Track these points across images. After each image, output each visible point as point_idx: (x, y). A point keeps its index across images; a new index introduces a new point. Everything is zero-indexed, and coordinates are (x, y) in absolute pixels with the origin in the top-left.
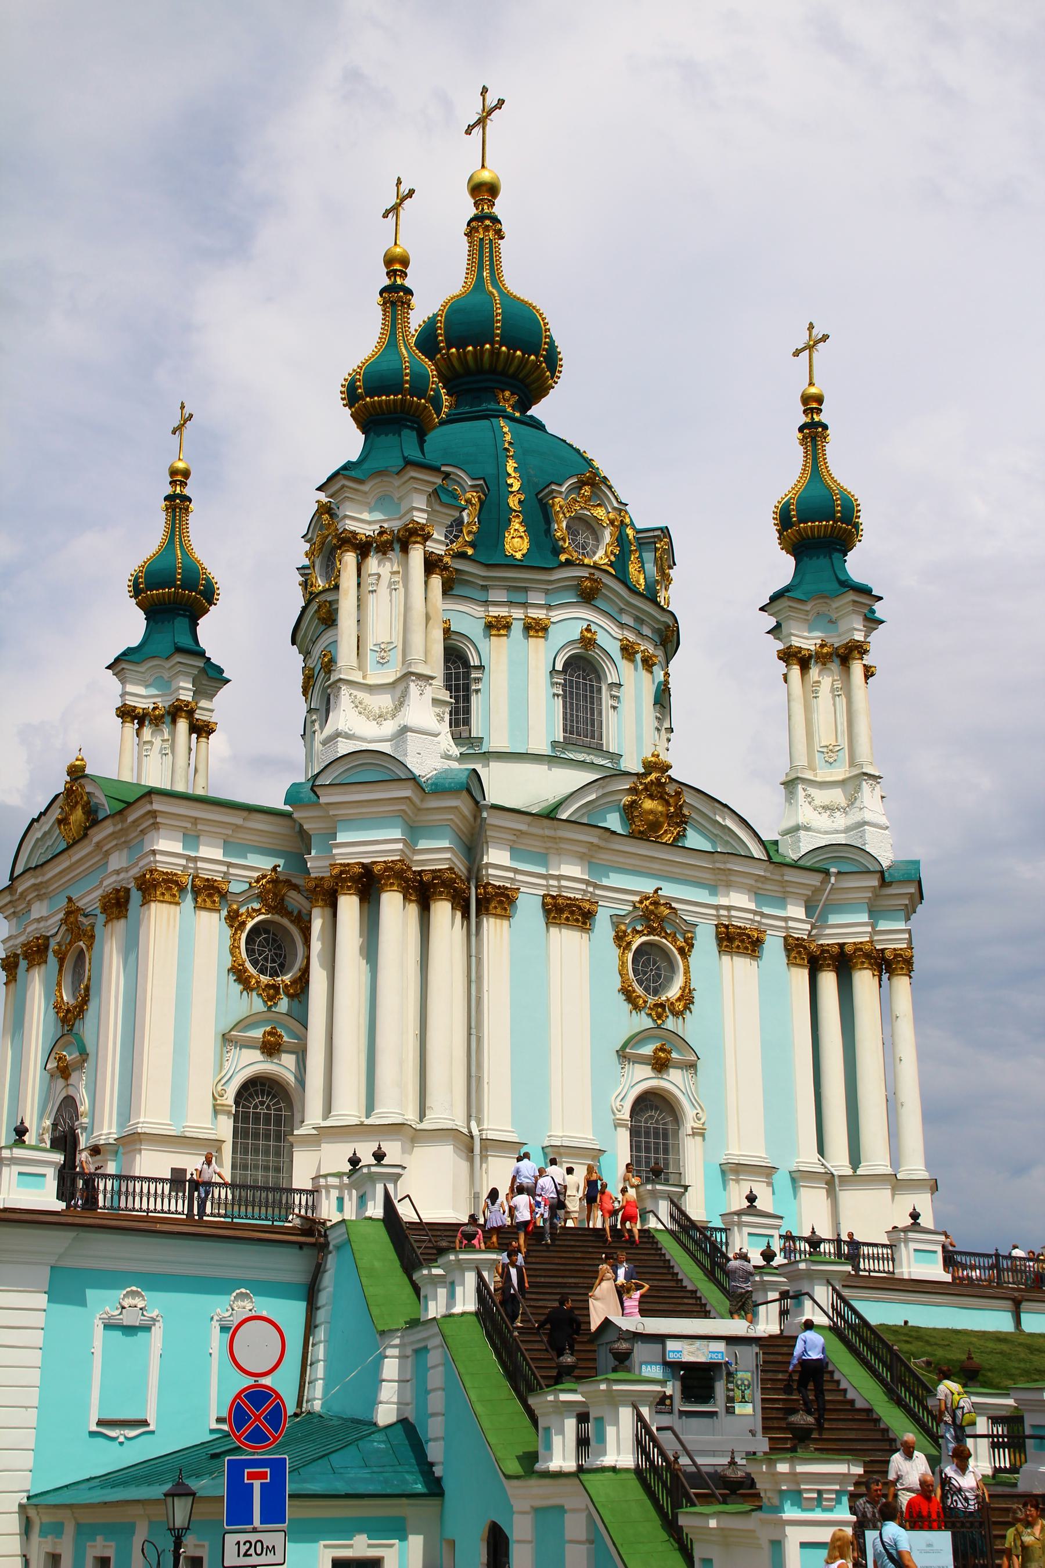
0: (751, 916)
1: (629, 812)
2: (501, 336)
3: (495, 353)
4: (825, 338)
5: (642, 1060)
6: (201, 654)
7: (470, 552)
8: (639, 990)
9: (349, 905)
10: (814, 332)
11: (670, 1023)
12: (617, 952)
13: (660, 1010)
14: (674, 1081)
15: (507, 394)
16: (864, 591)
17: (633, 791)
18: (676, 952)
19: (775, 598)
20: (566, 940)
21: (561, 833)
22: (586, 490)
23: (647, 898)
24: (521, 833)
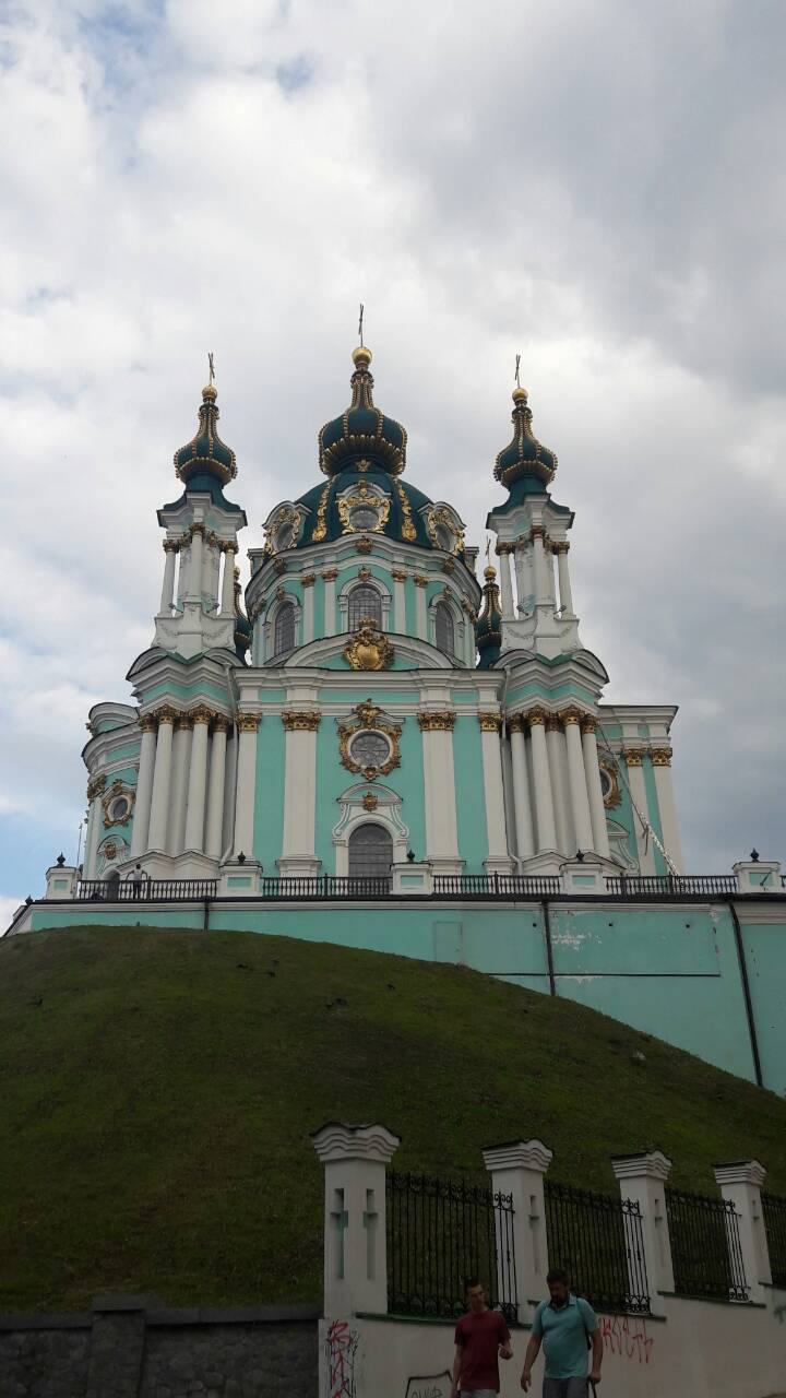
0: (443, 705)
3: (348, 440)
5: (354, 804)
7: (295, 545)
12: (339, 741)
13: (371, 774)
15: (363, 462)
17: (349, 643)
21: (288, 675)
22: (364, 490)
23: (362, 705)
24: (265, 680)
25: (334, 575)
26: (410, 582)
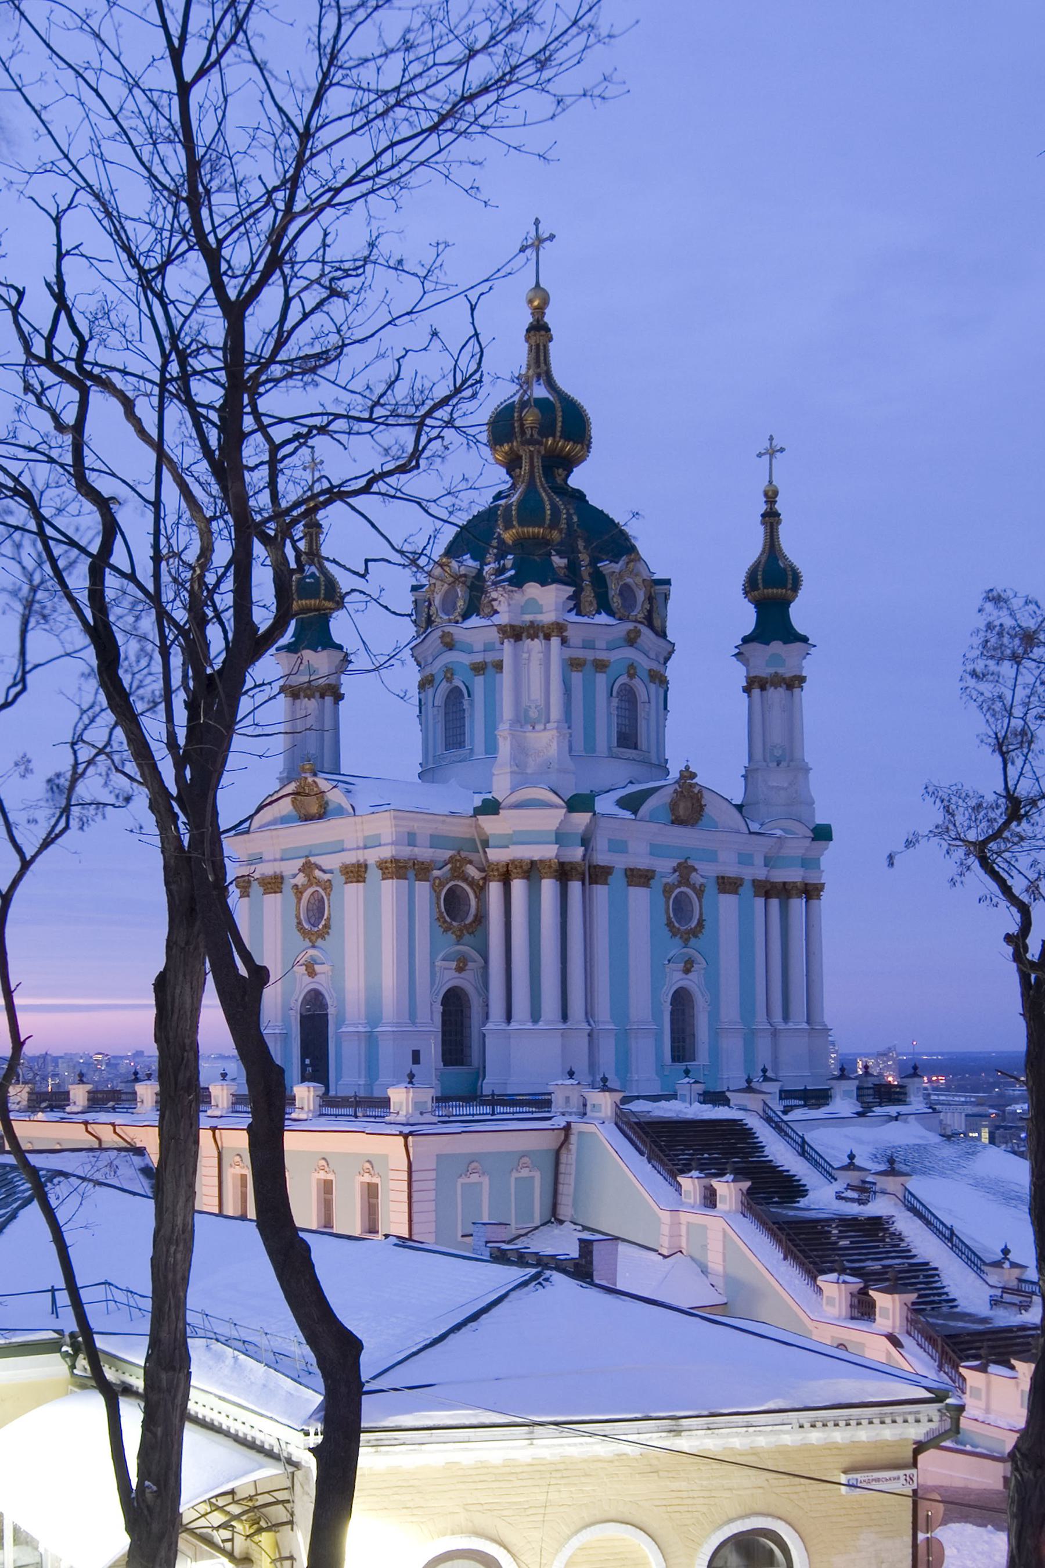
1: (673, 806)
2: (561, 432)
4: (782, 450)
6: (340, 647)
8: (676, 924)
9: (518, 886)
10: (774, 443)
11: (693, 941)
12: (662, 900)
14: (693, 982)
15: (560, 471)
16: (805, 640)
18: (694, 896)
19: (746, 640)
20: (639, 898)
25: (601, 666)
26: (657, 681)
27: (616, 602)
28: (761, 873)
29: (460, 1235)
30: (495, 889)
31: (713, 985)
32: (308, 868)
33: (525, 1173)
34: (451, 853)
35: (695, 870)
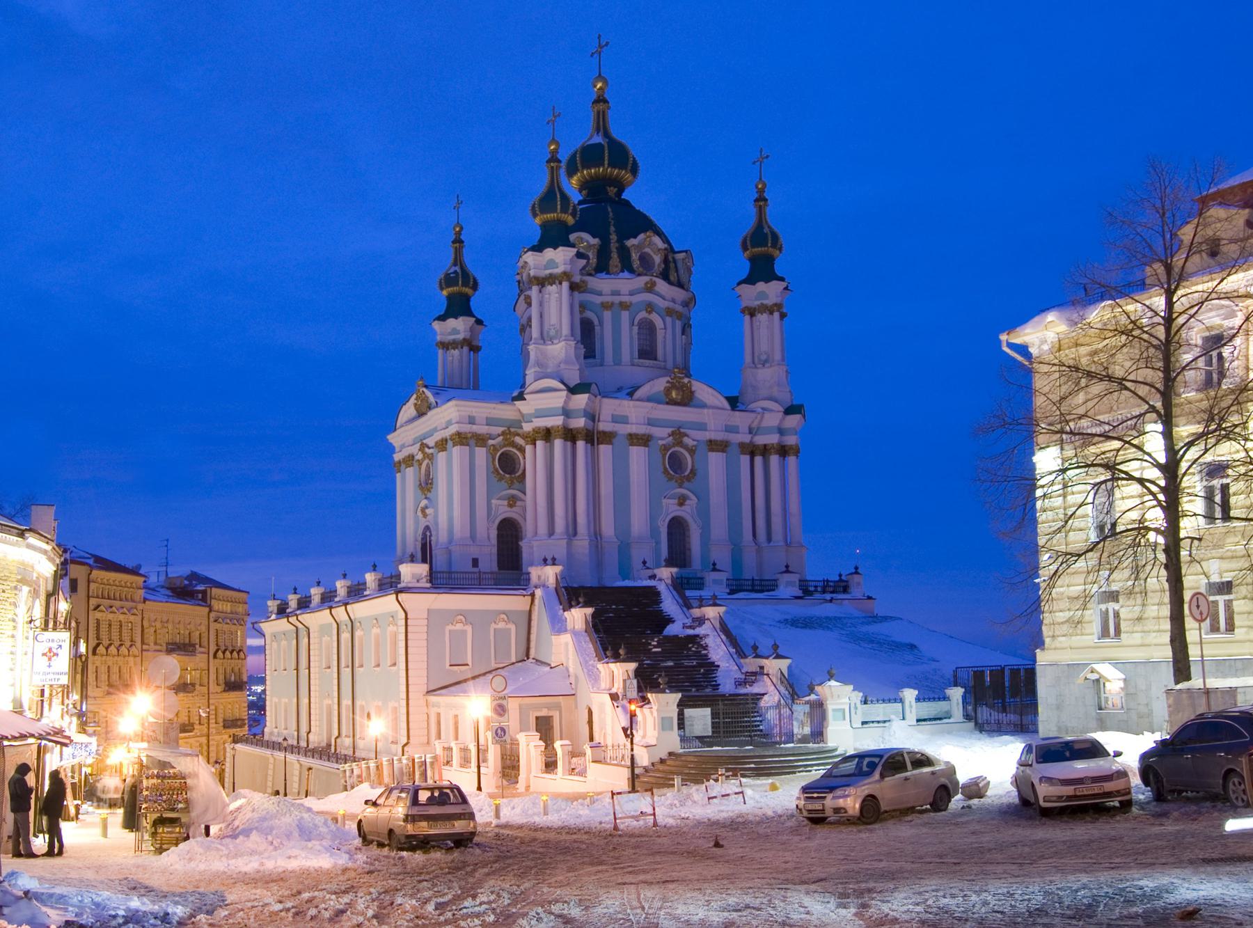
9: (539, 443)
11: (686, 484)
14: (686, 512)
20: (637, 455)
27: (636, 263)
28: (746, 439)
29: (448, 666)
30: (529, 448)
31: (704, 514)
32: (423, 446)
33: (501, 625)
34: (502, 429)
35: (687, 435)
